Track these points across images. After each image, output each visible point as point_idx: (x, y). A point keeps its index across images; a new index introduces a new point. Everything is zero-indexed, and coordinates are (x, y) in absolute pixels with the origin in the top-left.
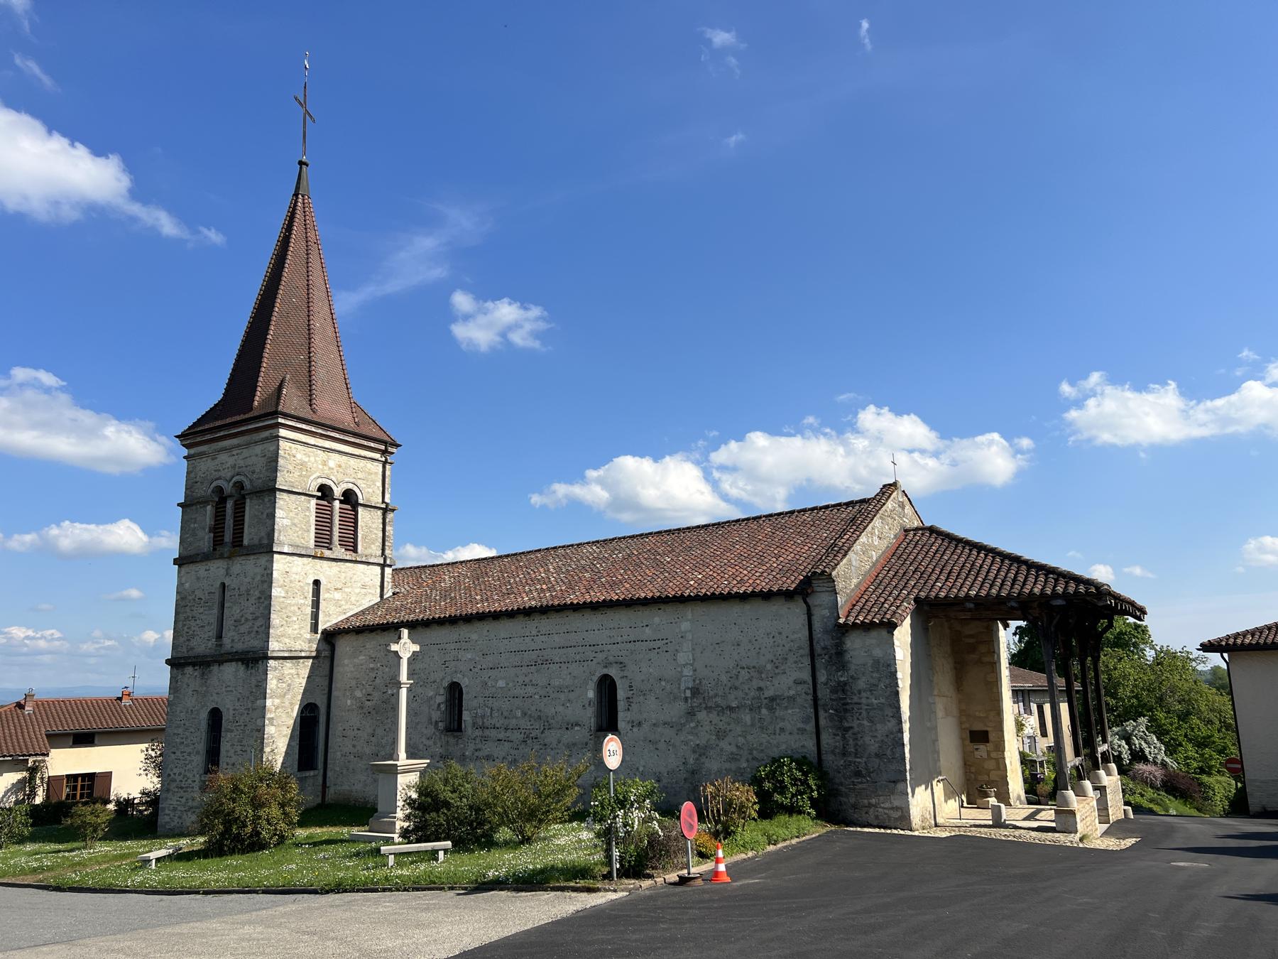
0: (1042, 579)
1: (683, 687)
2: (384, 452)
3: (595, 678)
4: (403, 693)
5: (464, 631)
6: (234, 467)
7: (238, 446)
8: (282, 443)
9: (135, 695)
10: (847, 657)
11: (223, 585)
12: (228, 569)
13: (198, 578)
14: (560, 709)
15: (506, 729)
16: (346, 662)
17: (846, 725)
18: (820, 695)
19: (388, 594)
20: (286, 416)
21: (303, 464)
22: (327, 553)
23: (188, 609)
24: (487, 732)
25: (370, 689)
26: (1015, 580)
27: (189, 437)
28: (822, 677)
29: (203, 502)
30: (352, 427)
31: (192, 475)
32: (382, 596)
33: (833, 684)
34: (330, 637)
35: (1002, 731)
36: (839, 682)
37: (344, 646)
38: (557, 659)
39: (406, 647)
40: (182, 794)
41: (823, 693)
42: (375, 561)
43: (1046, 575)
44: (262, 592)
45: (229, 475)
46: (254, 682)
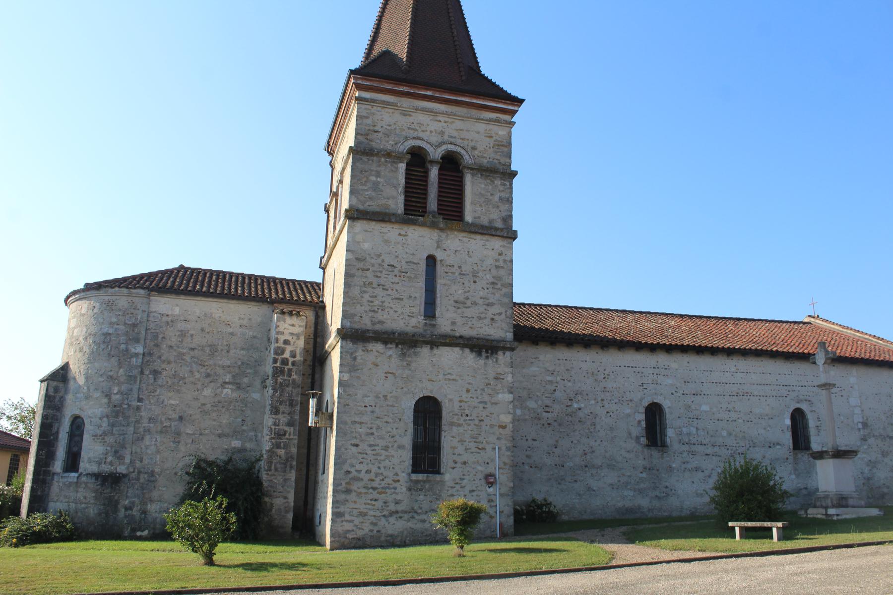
1: (856, 421)
3: (791, 410)
6: (442, 133)
14: (761, 431)
15: (713, 446)
23: (368, 274)
24: (694, 448)
25: (548, 402)
31: (369, 121)
38: (756, 393)
40: (375, 495)
45: (434, 139)
46: (491, 374)
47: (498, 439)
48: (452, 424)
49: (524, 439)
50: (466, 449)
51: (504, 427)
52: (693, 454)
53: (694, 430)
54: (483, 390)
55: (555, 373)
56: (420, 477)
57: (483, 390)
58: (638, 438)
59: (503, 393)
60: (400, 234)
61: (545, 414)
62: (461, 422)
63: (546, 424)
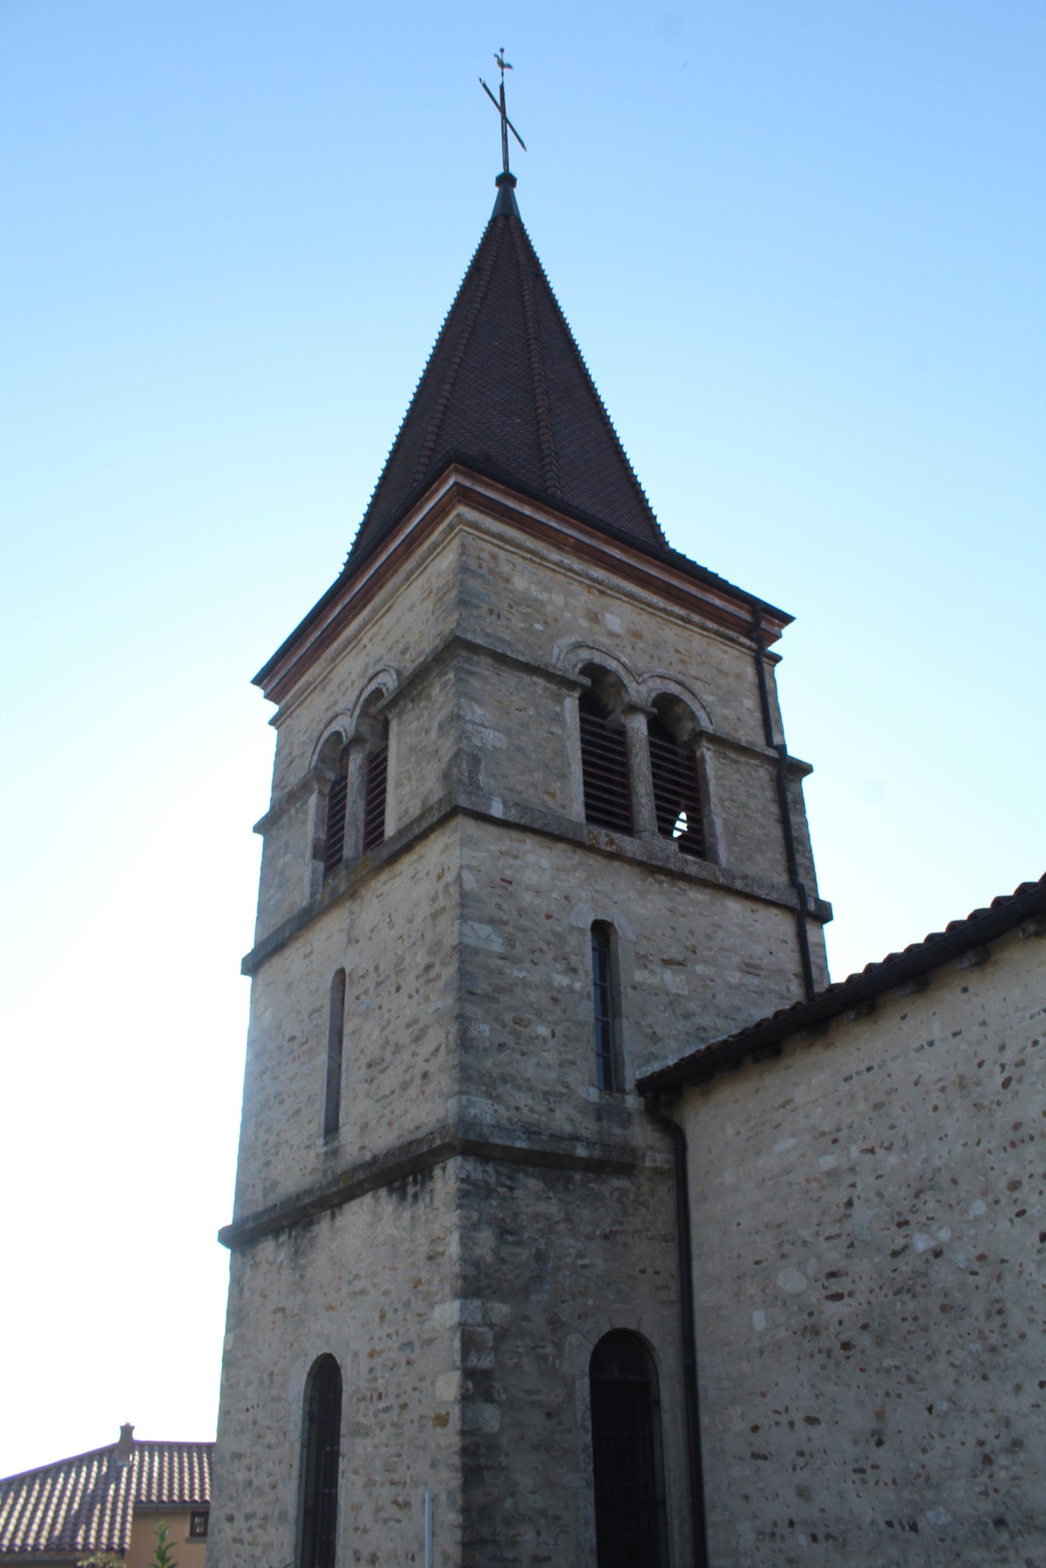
22: (628, 845)
25: (833, 1257)
42: (774, 896)
47: (433, 1465)
48: (361, 1431)
49: (784, 1419)
50: (379, 1509)
51: (441, 1421)
54: (408, 1304)
55: (842, 1136)
57: (408, 1304)
59: (442, 1301)
60: (306, 956)
61: (833, 1308)
62: (370, 1421)
63: (838, 1352)
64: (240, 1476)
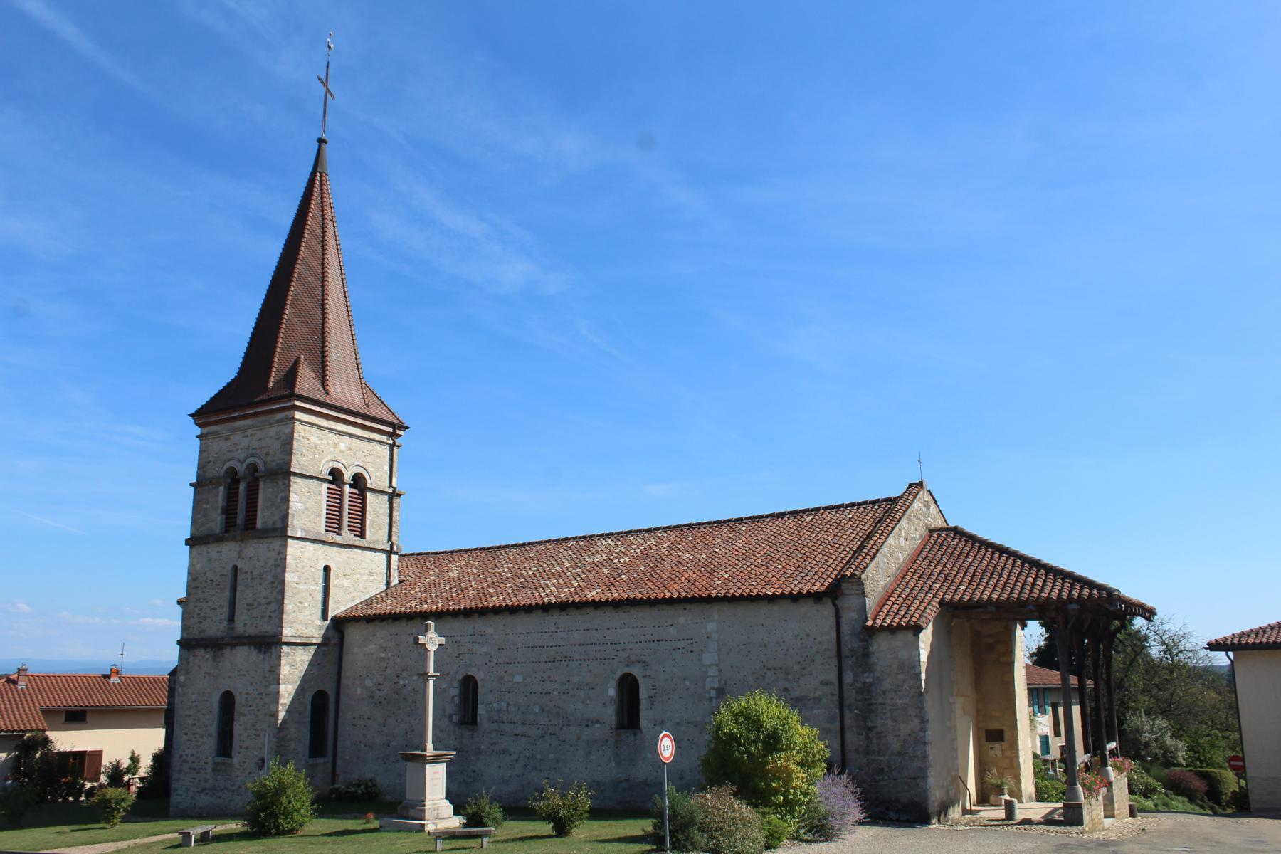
0: (1059, 583)
2: (393, 435)
3: (617, 676)
4: (431, 683)
5: (478, 624)
6: (248, 448)
7: (253, 426)
8: (297, 426)
9: (124, 674)
10: (873, 659)
11: (235, 568)
12: (240, 552)
13: (210, 560)
15: (524, 724)
16: (356, 650)
17: (870, 724)
18: (845, 696)
19: (394, 582)
20: (302, 398)
21: (315, 446)
25: (380, 680)
26: (1034, 584)
27: (203, 416)
28: (848, 678)
29: (214, 482)
30: (363, 410)
31: (205, 455)
32: (388, 583)
33: (859, 685)
34: (339, 626)
35: (1016, 729)
36: (864, 683)
37: (354, 635)
39: (432, 640)
41: (850, 694)
43: (1063, 580)
44: (276, 577)
45: (242, 456)
52: (501, 733)
53: (504, 705)
56: (220, 760)
58: (451, 716)
64: (190, 722)
